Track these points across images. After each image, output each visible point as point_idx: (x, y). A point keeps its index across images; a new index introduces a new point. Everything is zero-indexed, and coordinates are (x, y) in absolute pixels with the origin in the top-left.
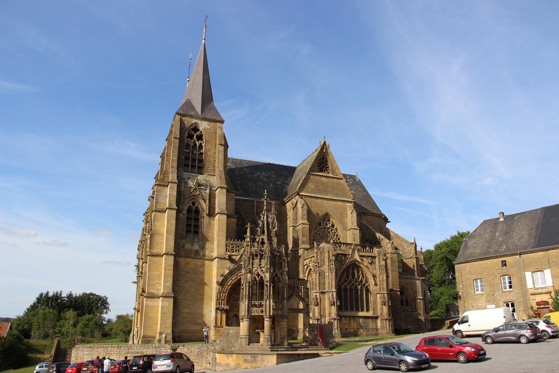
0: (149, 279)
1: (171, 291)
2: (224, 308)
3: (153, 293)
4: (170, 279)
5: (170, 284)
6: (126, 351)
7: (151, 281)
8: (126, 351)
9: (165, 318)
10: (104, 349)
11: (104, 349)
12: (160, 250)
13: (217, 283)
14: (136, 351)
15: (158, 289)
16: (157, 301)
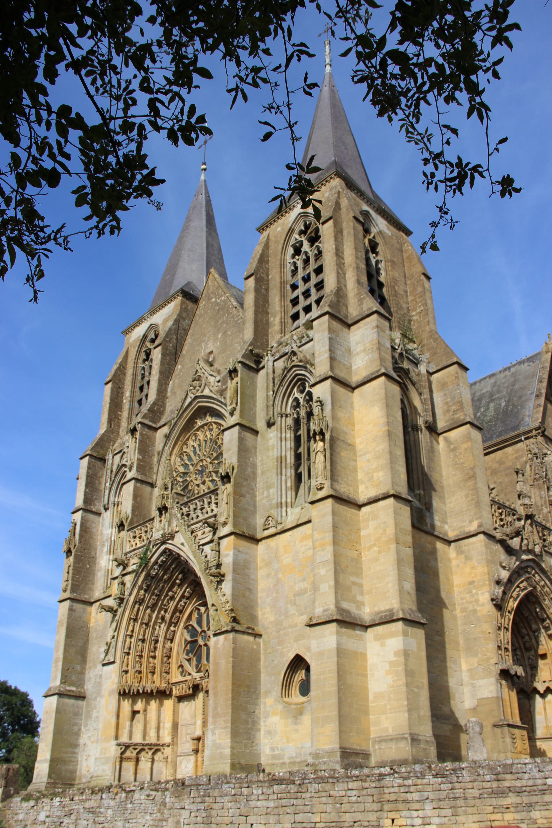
0: (338, 567)
1: (414, 608)
2: (516, 672)
3: (348, 612)
4: (410, 572)
5: (411, 587)
6: (488, 785)
7: (341, 576)
8: (488, 785)
9: (416, 690)
10: (366, 785)
11: (366, 785)
12: (351, 489)
13: (492, 600)
14: (539, 782)
15: (358, 602)
16: (360, 638)
